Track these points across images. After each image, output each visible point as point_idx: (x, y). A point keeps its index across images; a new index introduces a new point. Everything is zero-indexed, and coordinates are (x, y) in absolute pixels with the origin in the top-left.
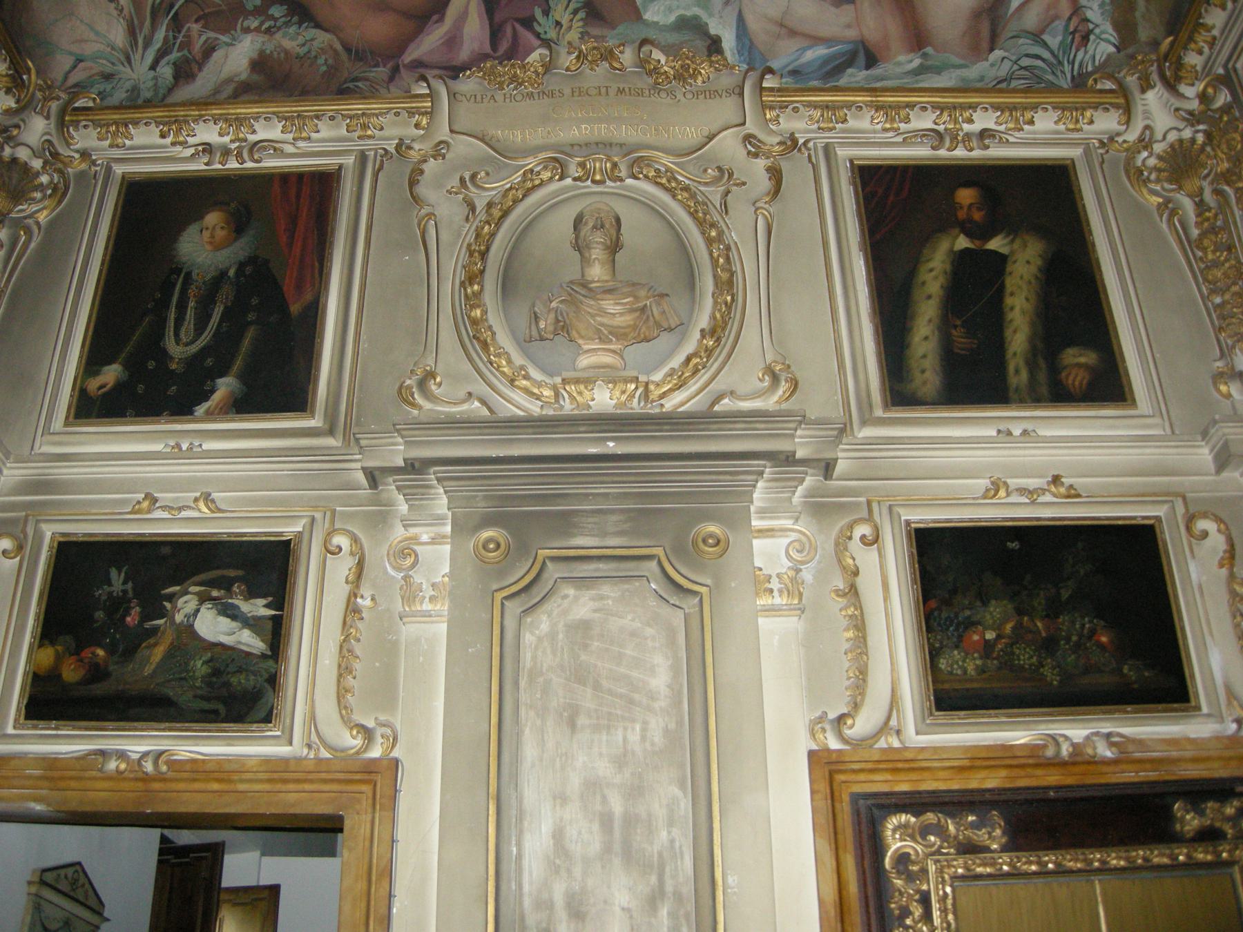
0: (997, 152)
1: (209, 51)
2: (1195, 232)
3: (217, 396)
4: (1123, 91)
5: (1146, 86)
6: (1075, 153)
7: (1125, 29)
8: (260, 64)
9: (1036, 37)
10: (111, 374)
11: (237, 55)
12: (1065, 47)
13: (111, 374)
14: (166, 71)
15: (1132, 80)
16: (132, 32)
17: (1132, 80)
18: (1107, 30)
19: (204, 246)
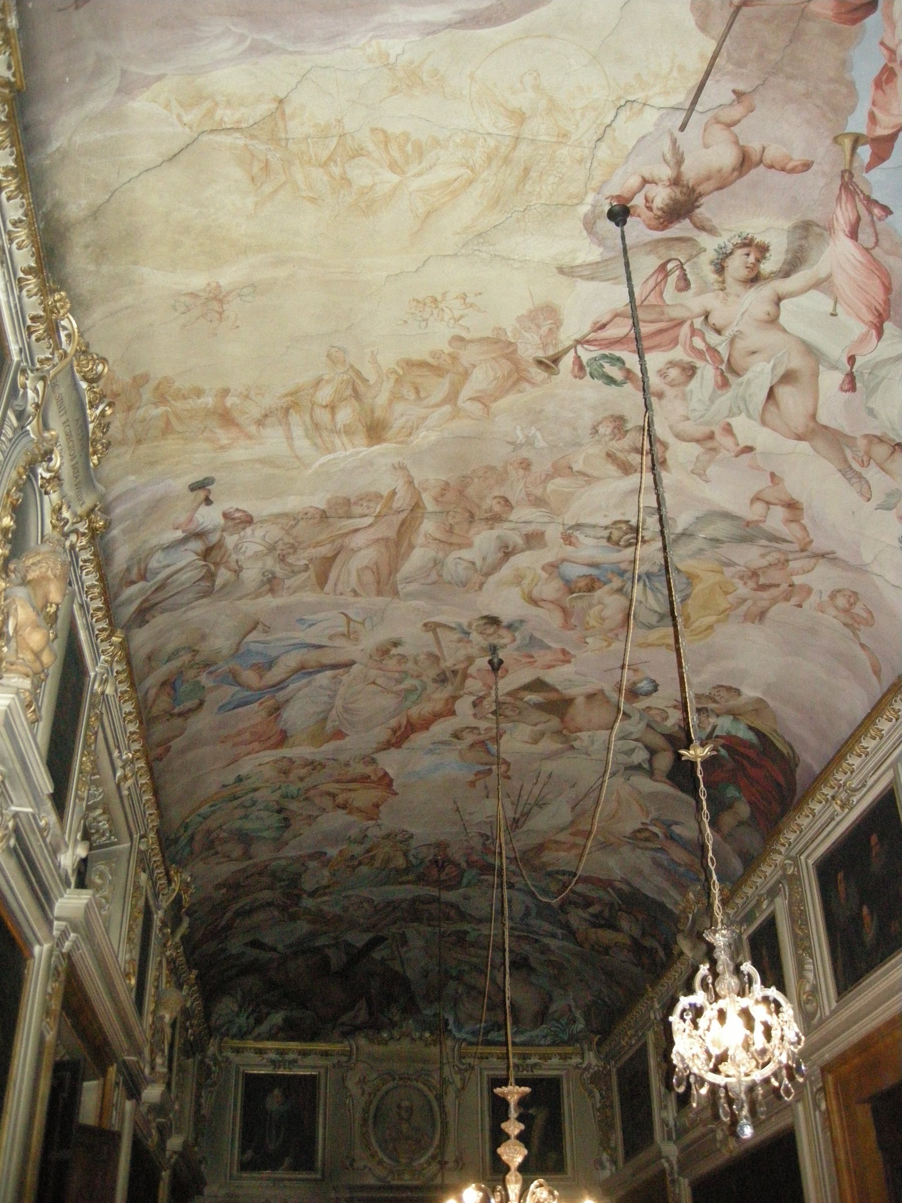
0: (538, 1072)
1: (268, 1014)
2: (598, 1105)
3: (286, 1164)
4: (582, 1049)
5: (590, 1049)
6: (563, 1073)
7: (588, 1021)
8: (285, 1020)
9: (557, 1021)
10: (249, 1154)
11: (277, 1018)
12: (567, 1024)
13: (249, 1154)
14: (252, 1020)
15: (586, 1046)
16: (240, 1007)
17: (586, 1046)
18: (582, 1020)
19: (274, 1102)
